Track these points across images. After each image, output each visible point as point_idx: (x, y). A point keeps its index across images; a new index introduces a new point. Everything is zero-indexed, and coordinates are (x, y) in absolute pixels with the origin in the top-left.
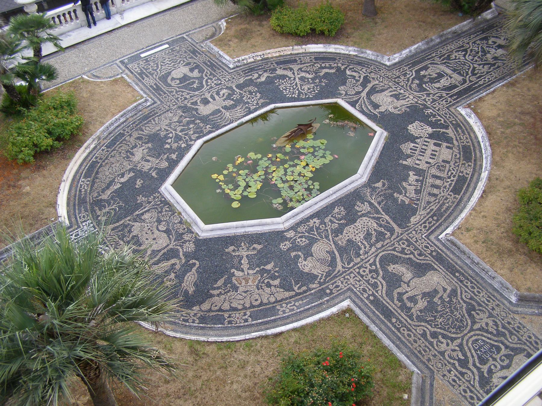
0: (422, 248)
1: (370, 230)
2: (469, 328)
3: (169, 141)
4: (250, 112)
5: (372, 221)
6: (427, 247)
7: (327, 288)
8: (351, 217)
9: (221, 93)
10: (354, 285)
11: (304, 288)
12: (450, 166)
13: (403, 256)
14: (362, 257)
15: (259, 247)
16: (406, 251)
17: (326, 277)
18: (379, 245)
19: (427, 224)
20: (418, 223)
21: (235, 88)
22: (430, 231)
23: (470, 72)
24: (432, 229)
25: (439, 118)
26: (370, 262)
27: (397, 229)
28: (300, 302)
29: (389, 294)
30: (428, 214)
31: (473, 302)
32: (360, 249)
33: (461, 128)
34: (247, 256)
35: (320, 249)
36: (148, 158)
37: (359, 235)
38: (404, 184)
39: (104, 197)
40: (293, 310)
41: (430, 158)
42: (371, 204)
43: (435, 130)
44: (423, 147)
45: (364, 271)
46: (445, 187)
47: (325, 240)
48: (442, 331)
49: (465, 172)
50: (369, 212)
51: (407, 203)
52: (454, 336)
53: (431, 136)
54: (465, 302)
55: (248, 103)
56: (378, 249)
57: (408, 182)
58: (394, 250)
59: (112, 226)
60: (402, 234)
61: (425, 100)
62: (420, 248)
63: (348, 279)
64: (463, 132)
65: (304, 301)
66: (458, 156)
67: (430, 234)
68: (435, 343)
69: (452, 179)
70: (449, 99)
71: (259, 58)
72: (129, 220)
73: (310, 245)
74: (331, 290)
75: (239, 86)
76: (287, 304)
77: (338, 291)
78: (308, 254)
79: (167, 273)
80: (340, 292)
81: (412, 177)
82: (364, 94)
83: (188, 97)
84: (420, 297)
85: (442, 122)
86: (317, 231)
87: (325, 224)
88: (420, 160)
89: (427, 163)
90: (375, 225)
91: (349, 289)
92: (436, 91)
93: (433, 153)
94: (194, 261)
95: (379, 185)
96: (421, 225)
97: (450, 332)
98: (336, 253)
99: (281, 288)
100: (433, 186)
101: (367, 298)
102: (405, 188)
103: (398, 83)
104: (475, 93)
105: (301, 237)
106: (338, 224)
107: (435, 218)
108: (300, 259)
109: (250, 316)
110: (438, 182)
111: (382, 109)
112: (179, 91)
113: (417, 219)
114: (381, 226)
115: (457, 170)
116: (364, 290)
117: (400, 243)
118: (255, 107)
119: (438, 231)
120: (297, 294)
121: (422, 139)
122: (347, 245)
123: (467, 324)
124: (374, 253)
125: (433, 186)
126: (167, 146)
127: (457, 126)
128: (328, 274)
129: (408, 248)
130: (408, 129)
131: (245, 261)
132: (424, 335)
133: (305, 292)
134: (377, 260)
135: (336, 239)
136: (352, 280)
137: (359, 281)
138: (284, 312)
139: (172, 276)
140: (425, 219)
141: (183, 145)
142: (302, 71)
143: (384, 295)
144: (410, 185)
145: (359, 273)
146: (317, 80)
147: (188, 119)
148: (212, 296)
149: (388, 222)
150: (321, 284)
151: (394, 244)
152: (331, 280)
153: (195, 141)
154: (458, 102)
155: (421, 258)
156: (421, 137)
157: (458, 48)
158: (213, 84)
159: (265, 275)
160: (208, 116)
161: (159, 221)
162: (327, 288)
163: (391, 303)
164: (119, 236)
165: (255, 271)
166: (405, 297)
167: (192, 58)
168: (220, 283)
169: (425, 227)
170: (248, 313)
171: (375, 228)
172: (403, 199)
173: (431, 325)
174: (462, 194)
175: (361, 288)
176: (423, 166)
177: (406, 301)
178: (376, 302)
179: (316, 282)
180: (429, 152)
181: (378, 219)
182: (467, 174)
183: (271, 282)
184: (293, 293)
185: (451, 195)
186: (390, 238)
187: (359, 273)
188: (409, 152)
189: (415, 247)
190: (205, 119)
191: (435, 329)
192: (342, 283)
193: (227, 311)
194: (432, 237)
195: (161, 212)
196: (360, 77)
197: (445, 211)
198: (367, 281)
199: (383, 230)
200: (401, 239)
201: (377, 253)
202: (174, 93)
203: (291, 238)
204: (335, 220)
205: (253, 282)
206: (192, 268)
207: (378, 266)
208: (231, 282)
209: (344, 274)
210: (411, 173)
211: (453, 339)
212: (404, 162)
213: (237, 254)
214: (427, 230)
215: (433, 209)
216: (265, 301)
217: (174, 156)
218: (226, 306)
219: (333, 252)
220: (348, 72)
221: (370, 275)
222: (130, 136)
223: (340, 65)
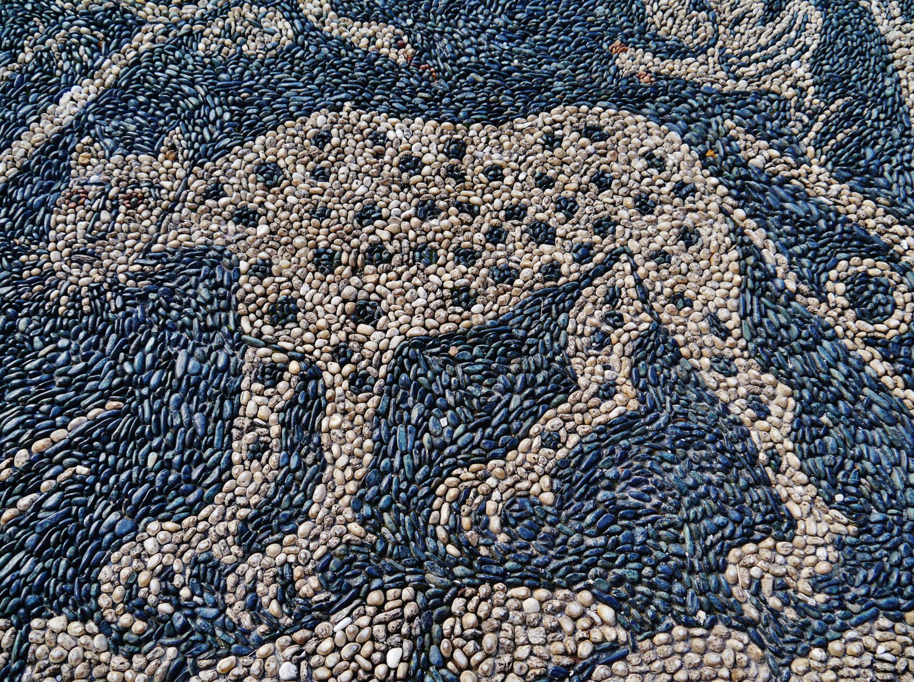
1: (588, 315)
5: (714, 214)
50: (764, 114)
122: (91, 319)
171: (688, 328)
199: (773, 431)
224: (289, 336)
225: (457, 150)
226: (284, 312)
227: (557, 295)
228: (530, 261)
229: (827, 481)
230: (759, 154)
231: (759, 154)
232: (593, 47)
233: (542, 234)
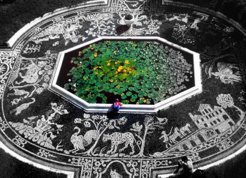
0: (142, 174)
1: (126, 143)
3: (91, 29)
4: (143, 35)
7: (71, 158)
8: (125, 129)
10: (84, 167)
11: (61, 150)
12: (217, 136)
15: (66, 112)
17: (78, 152)
18: (121, 155)
20: (157, 158)
22: (158, 168)
24: (160, 167)
27: (141, 153)
28: (52, 156)
30: (169, 157)
32: (110, 149)
34: (57, 113)
35: (90, 135)
37: (118, 141)
38: (176, 129)
39: (37, 42)
41: (211, 123)
42: (144, 127)
43: (235, 107)
44: (215, 114)
45: (98, 164)
46: (198, 148)
47: (99, 131)
50: (137, 133)
51: (164, 142)
56: (119, 157)
57: (179, 129)
58: (126, 164)
59: (24, 58)
60: (140, 158)
62: (140, 174)
63: (85, 161)
65: (54, 157)
66: (230, 133)
67: (155, 170)
69: (209, 145)
72: (33, 60)
73: (89, 129)
74: (72, 161)
76: (46, 151)
77: (74, 164)
78: (83, 133)
79: (18, 97)
80: (74, 165)
81: (186, 127)
83: (124, 10)
86: (100, 124)
87: (109, 122)
88: (203, 120)
89: (206, 125)
90: (132, 142)
91: (80, 168)
93: (217, 121)
95: (161, 120)
96: (157, 160)
98: (96, 142)
99: (52, 141)
102: (173, 131)
105: (89, 121)
106: (115, 127)
107: (170, 162)
108: (76, 133)
110: (198, 142)
111: (216, 74)
112: (124, 5)
114: (134, 144)
115: (219, 142)
118: (149, 33)
120: (55, 150)
121: (219, 108)
122: (106, 142)
124: (114, 157)
126: (87, 32)
128: (81, 151)
129: (134, 168)
130: (218, 96)
131: (53, 115)
133: (60, 152)
135: (104, 135)
136: (87, 163)
137: (89, 167)
138: (40, 154)
139: (18, 100)
140: (164, 159)
141: (94, 36)
144: (179, 132)
145: (94, 162)
147: (111, 22)
148: (22, 122)
149: (140, 146)
150: (71, 154)
151: (129, 160)
152: (77, 155)
153: (101, 36)
156: (220, 106)
159: (53, 129)
161: (43, 69)
162: (71, 158)
164: (21, 65)
165: (51, 124)
170: (26, 143)
171: (131, 144)
172: (165, 138)
174: (204, 159)
175: (86, 171)
176: (200, 125)
179: (70, 151)
180: (214, 119)
182: (222, 148)
184: (53, 148)
185: (196, 155)
186: (132, 155)
187: (94, 162)
189: (139, 171)
192: (81, 161)
193: (19, 134)
194: (155, 173)
195: (48, 64)
196: (226, 46)
198: (93, 170)
199: (133, 148)
200: (137, 161)
201: (115, 159)
202: (120, 4)
203: (85, 119)
204: (115, 124)
206: (30, 102)
207: (108, 166)
209: (87, 158)
210: (188, 125)
212: (191, 116)
214: (157, 166)
215: (175, 156)
216: (38, 143)
217: (84, 39)
219: (95, 141)
220: (223, 40)
221: (98, 168)
222: (79, 17)
224: (114, 144)
225: (121, 135)
226: (113, 143)
227: (125, 142)
228: (124, 140)
229: (134, 151)
230: (136, 135)
231: (136, 135)
232: (129, 129)
233: (125, 139)
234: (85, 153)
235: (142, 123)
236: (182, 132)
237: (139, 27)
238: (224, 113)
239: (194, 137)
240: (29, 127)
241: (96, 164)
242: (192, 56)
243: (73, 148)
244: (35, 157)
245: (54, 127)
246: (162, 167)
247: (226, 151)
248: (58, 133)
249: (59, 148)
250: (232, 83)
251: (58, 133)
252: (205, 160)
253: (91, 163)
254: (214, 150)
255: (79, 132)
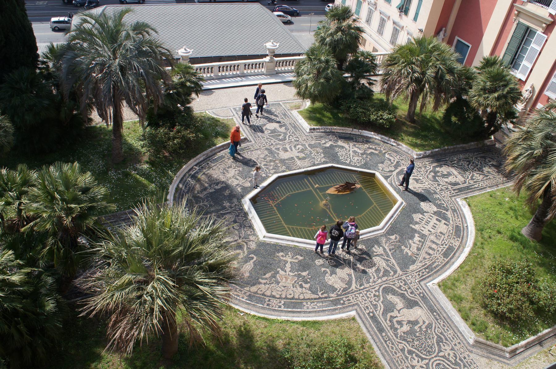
2: (435, 354)
4: (314, 165)
6: (418, 289)
7: (342, 299)
9: (297, 147)
11: (326, 295)
13: (400, 291)
14: (370, 284)
15: (301, 258)
16: (402, 288)
17: (343, 291)
18: (384, 279)
19: (421, 273)
21: (307, 146)
23: (470, 177)
25: (443, 202)
26: (376, 289)
27: (399, 272)
28: (321, 304)
29: (385, 313)
30: (423, 266)
31: (442, 336)
32: (371, 278)
33: (457, 213)
34: (291, 263)
36: (238, 177)
38: (410, 241)
40: (315, 308)
42: (384, 248)
44: (429, 219)
45: (370, 294)
48: (416, 351)
49: (454, 244)
50: (382, 255)
52: (424, 356)
53: (435, 213)
54: (437, 335)
55: (314, 158)
60: (402, 275)
61: (435, 188)
64: (458, 216)
66: (451, 232)
68: (410, 358)
69: (444, 246)
70: (452, 192)
71: (328, 131)
74: (344, 301)
75: (310, 145)
76: (311, 303)
81: (417, 238)
82: (394, 173)
84: (405, 323)
85: (445, 206)
89: (429, 231)
90: (385, 264)
91: (357, 304)
92: (445, 184)
94: (253, 255)
95: (393, 237)
97: (422, 353)
100: (430, 248)
101: (368, 314)
103: (420, 172)
104: (471, 192)
107: (427, 270)
109: (283, 304)
110: (434, 246)
113: (414, 268)
114: (388, 265)
116: (367, 307)
117: (399, 281)
119: (428, 280)
120: (320, 298)
123: (435, 350)
125: (430, 248)
127: (454, 211)
131: (288, 265)
132: (403, 350)
133: (326, 298)
134: (381, 289)
136: (360, 298)
138: (308, 308)
142: (355, 147)
143: (381, 315)
144: (414, 243)
145: (366, 294)
146: (365, 156)
148: (260, 283)
150: (338, 295)
151: (394, 281)
152: (346, 294)
153: (273, 174)
154: (458, 195)
155: (411, 295)
156: (428, 212)
157: (466, 159)
158: (293, 140)
160: (284, 160)
163: (384, 321)
166: (395, 320)
167: (282, 118)
168: (268, 275)
169: (419, 275)
170: (283, 302)
173: (409, 345)
174: (449, 258)
176: (426, 232)
177: (395, 323)
178: (374, 318)
180: (431, 224)
181: (387, 260)
183: (304, 285)
188: (418, 220)
190: (283, 161)
191: (412, 349)
192: (353, 298)
193: (268, 296)
194: (422, 283)
195: (238, 216)
196: (394, 161)
197: (435, 268)
198: (371, 302)
199: (389, 269)
200: (401, 279)
205: (291, 280)
207: (381, 293)
208: (275, 277)
210: (417, 235)
211: (422, 359)
212: (413, 227)
213: (284, 259)
214: (420, 277)
216: (296, 297)
218: (268, 293)
219: (351, 275)
220: (387, 156)
221: (373, 298)
223: (382, 149)
234: (351, 289)
235: (379, 245)
236: (418, 243)
237: (304, 158)
238: (435, 217)
239: (428, 243)
240: (272, 285)
241: (368, 295)
242: (373, 175)
243: (337, 289)
244: (305, 312)
245: (299, 276)
246: (424, 277)
247: (459, 247)
248: (308, 280)
249: (322, 294)
250: (423, 191)
251: (308, 280)
252: (451, 259)
253: (363, 296)
254: (450, 249)
255: (329, 272)
